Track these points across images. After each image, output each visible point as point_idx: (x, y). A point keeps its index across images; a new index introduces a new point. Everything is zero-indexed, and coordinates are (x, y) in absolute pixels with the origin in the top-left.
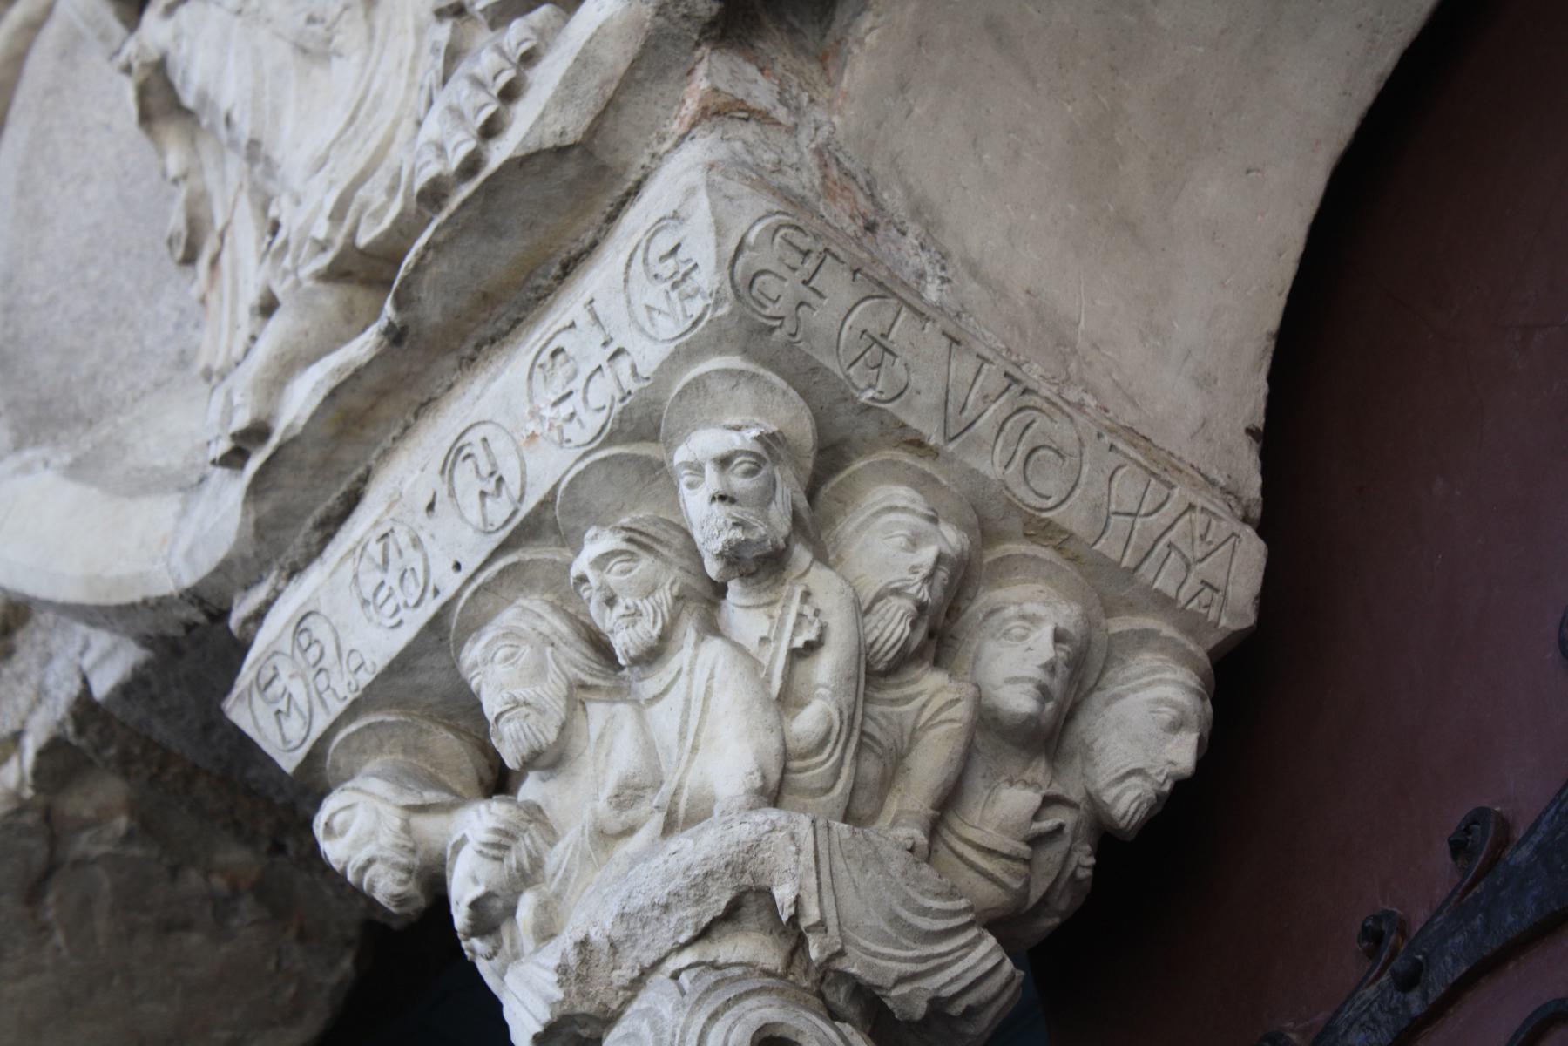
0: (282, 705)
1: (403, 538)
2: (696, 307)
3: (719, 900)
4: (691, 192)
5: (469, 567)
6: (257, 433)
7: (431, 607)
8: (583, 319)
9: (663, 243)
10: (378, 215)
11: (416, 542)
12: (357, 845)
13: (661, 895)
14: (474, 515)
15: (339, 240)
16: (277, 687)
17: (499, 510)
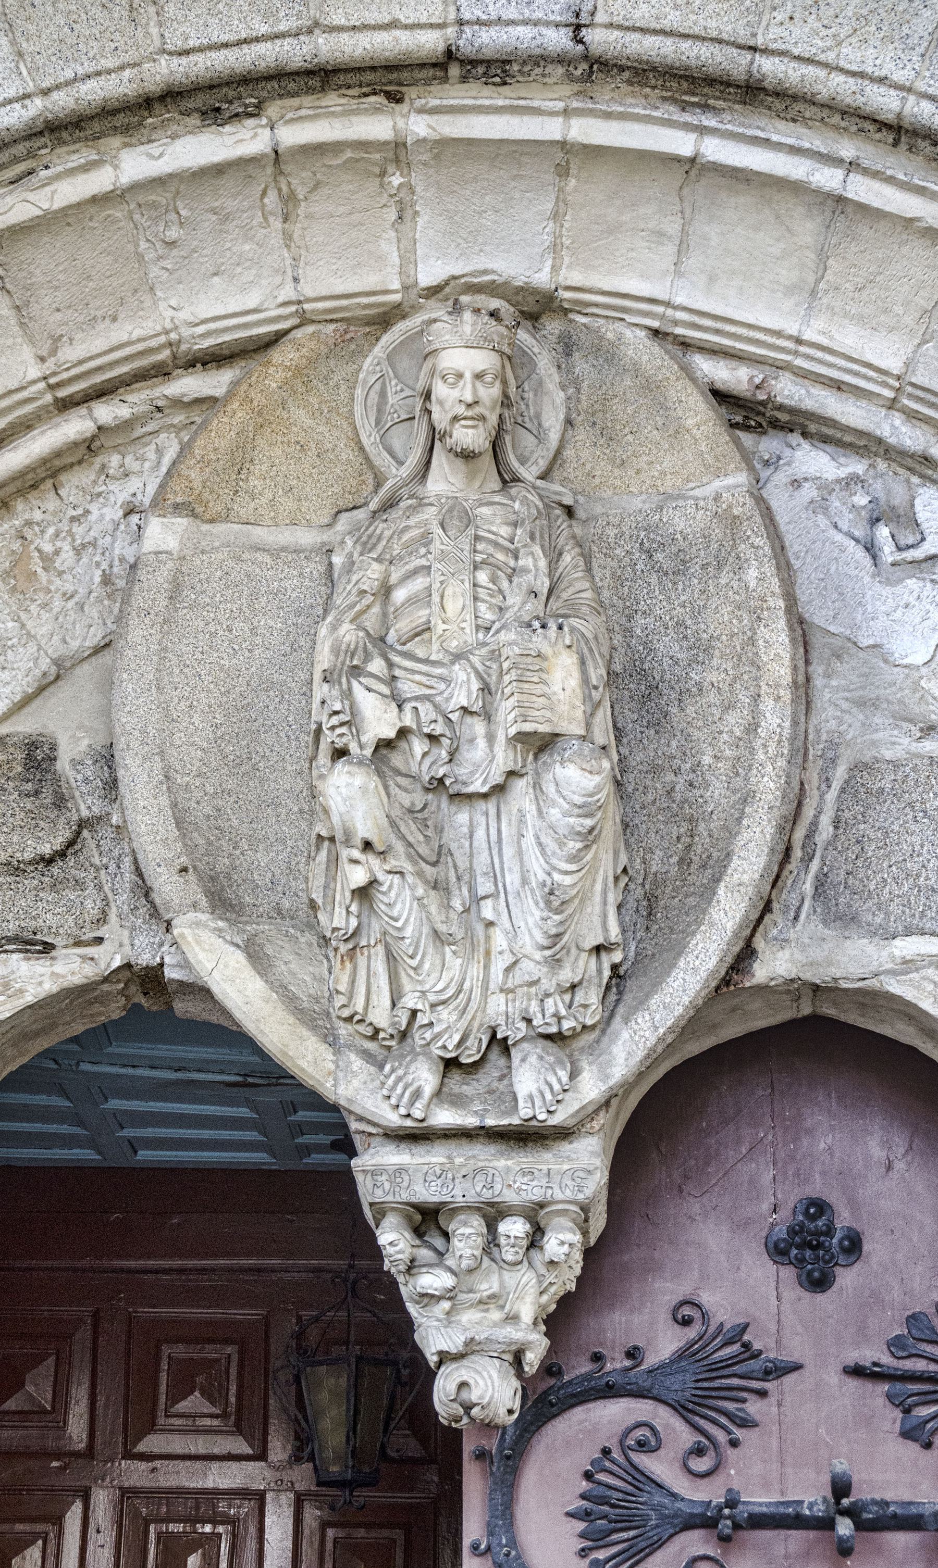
0: (379, 1184)
1: (450, 1176)
2: (581, 1196)
3: (514, 1348)
4: (596, 1168)
5: (467, 1199)
6: (422, 1121)
7: (450, 1200)
8: (546, 1171)
9: (582, 1174)
10: (470, 1056)
11: (453, 1179)
12: (398, 1252)
13: (501, 1340)
14: (478, 1189)
15: (453, 1055)
16: (379, 1178)
17: (487, 1195)
